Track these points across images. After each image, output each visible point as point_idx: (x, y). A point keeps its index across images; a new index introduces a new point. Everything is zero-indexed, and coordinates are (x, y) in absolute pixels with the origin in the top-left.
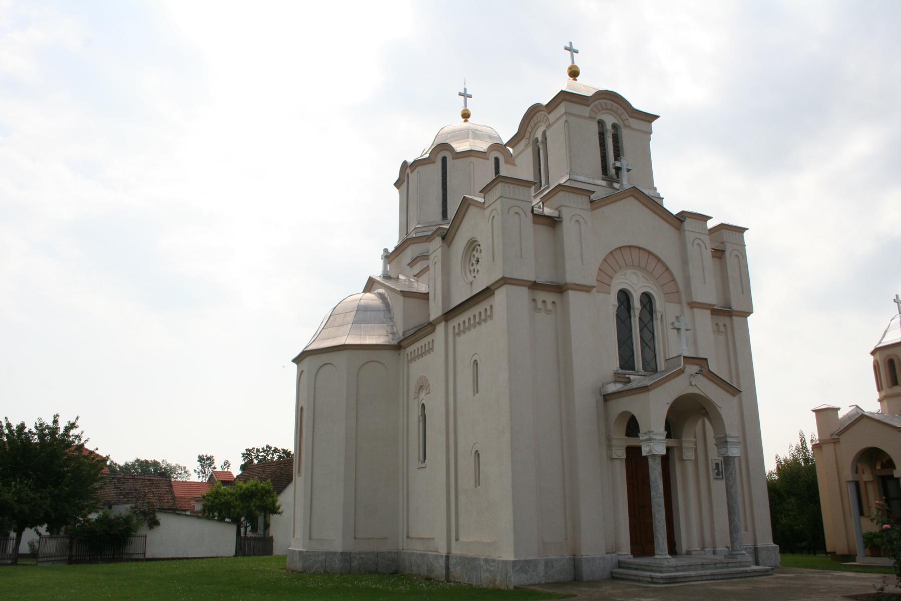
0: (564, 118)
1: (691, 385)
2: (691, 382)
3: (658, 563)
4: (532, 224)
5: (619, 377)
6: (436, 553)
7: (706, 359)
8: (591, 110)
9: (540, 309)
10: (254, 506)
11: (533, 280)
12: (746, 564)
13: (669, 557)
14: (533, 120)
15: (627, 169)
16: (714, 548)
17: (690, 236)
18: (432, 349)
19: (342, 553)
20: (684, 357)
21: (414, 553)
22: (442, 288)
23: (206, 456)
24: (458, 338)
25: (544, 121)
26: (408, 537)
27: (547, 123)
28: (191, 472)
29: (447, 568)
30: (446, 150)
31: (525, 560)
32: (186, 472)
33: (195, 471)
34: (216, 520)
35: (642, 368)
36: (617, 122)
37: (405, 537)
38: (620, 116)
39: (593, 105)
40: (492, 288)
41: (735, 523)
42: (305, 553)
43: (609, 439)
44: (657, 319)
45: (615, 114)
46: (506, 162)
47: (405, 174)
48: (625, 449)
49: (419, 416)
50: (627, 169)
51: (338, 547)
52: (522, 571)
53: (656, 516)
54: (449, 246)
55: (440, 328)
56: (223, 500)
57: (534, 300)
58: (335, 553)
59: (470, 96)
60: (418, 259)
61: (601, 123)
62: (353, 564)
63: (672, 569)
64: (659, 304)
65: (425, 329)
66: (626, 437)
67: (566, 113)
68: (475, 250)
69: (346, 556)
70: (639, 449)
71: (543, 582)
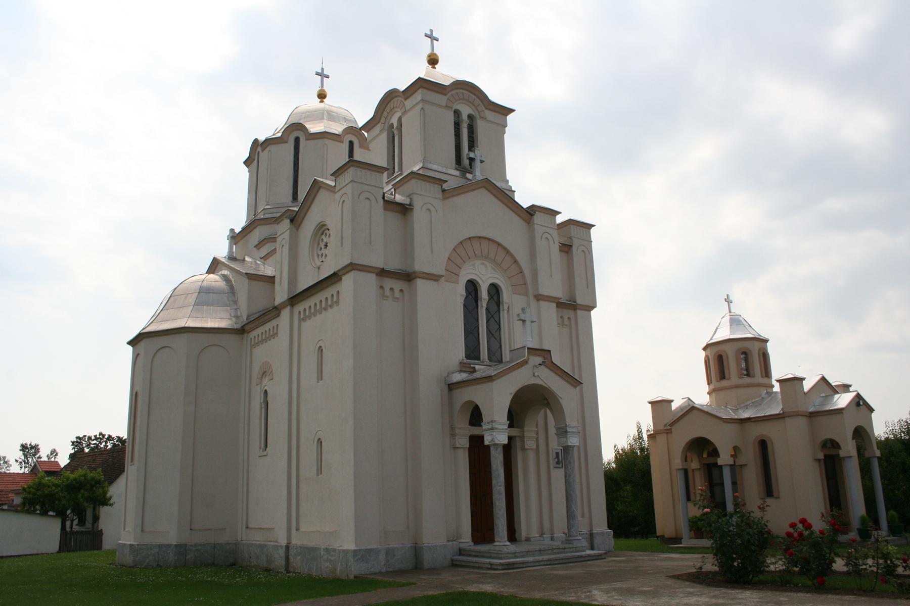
0: (420, 106)
1: (534, 376)
2: (534, 373)
3: (497, 549)
4: (382, 211)
5: (463, 366)
6: (276, 544)
7: (549, 351)
8: (448, 99)
9: (388, 297)
10: (82, 497)
11: (381, 266)
13: (509, 543)
14: (389, 105)
15: (481, 160)
16: (552, 534)
17: (539, 230)
18: (277, 334)
19: (176, 546)
20: (528, 348)
21: (253, 544)
22: (289, 272)
23: (30, 445)
24: (304, 325)
25: (400, 107)
26: (247, 527)
27: (403, 110)
28: (12, 462)
29: (287, 558)
30: (302, 131)
31: (366, 549)
32: (5, 462)
33: (16, 461)
34: (38, 514)
35: (487, 357)
36: (472, 112)
37: (244, 527)
38: (476, 107)
39: (450, 94)
40: (340, 273)
42: (137, 546)
43: (452, 428)
44: (503, 310)
45: (471, 105)
46: (361, 146)
47: (255, 153)
48: (468, 438)
49: (261, 403)
50: (481, 160)
51: (173, 539)
52: (363, 560)
53: (497, 504)
54: (297, 229)
55: (286, 313)
56: (46, 492)
57: (381, 287)
58: (169, 546)
59: (327, 77)
60: (266, 241)
61: (457, 113)
62: (187, 557)
63: (511, 555)
64: (506, 296)
65: (270, 313)
66: (470, 426)
67: (422, 100)
68: (324, 234)
69: (181, 549)
70: (481, 438)
71: (384, 571)
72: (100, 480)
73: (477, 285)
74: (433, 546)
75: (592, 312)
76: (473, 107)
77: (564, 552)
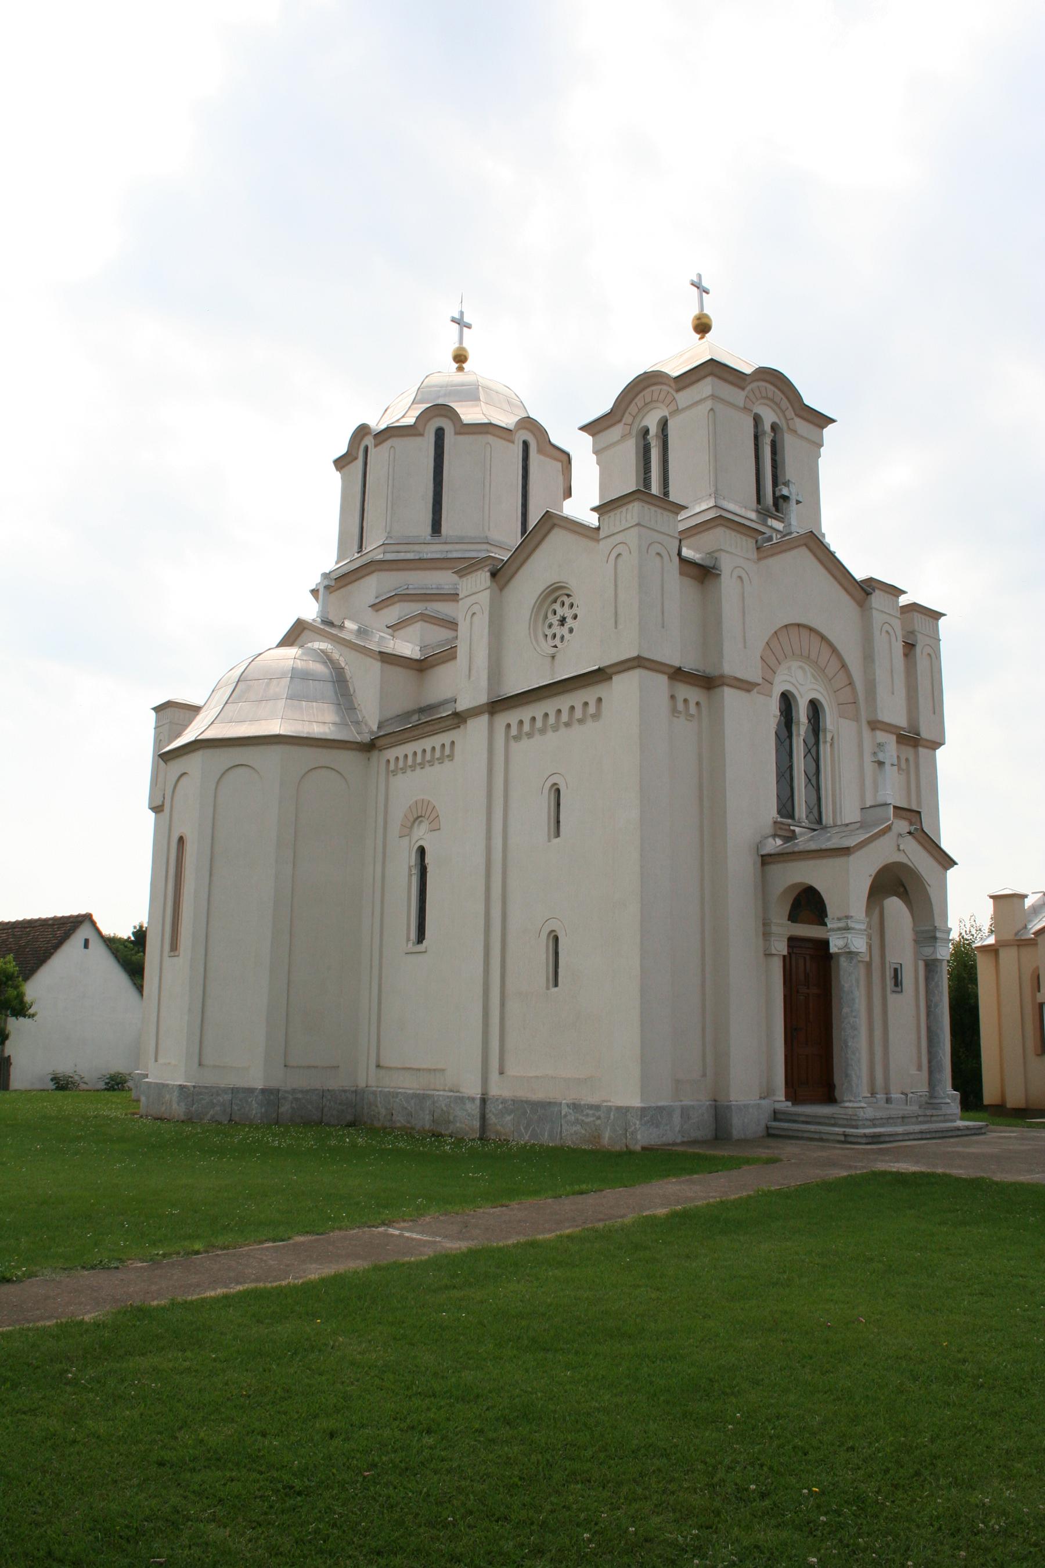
0: (709, 404)
1: (899, 850)
2: (899, 846)
3: (850, 1113)
4: (677, 575)
5: (781, 829)
6: (457, 1094)
7: (919, 813)
9: (680, 712)
11: (677, 664)
12: (951, 1118)
14: (642, 394)
15: (797, 501)
16: (886, 1094)
17: (877, 618)
19: (263, 1091)
20: (895, 807)
21: (398, 1094)
25: (667, 401)
26: (378, 1066)
27: (673, 407)
29: (483, 1118)
31: (657, 1107)
35: (804, 817)
36: (777, 421)
37: (373, 1066)
38: (783, 412)
39: (749, 388)
40: (609, 671)
41: (939, 1058)
42: (192, 1089)
43: (766, 924)
44: (825, 742)
45: (775, 407)
46: (540, 451)
47: (359, 445)
48: (786, 940)
50: (797, 501)
51: (257, 1082)
52: (653, 1124)
53: (850, 1044)
54: (501, 589)
58: (250, 1091)
59: (469, 326)
60: (396, 599)
61: (757, 420)
62: (282, 1110)
64: (830, 720)
65: (439, 722)
66: (790, 922)
67: (713, 397)
68: (559, 601)
69: (271, 1096)
70: (826, 943)
71: (679, 1141)
72: (13, 974)
73: (791, 699)
74: (745, 1106)
75: (937, 751)
76: (778, 411)
77: (931, 1122)
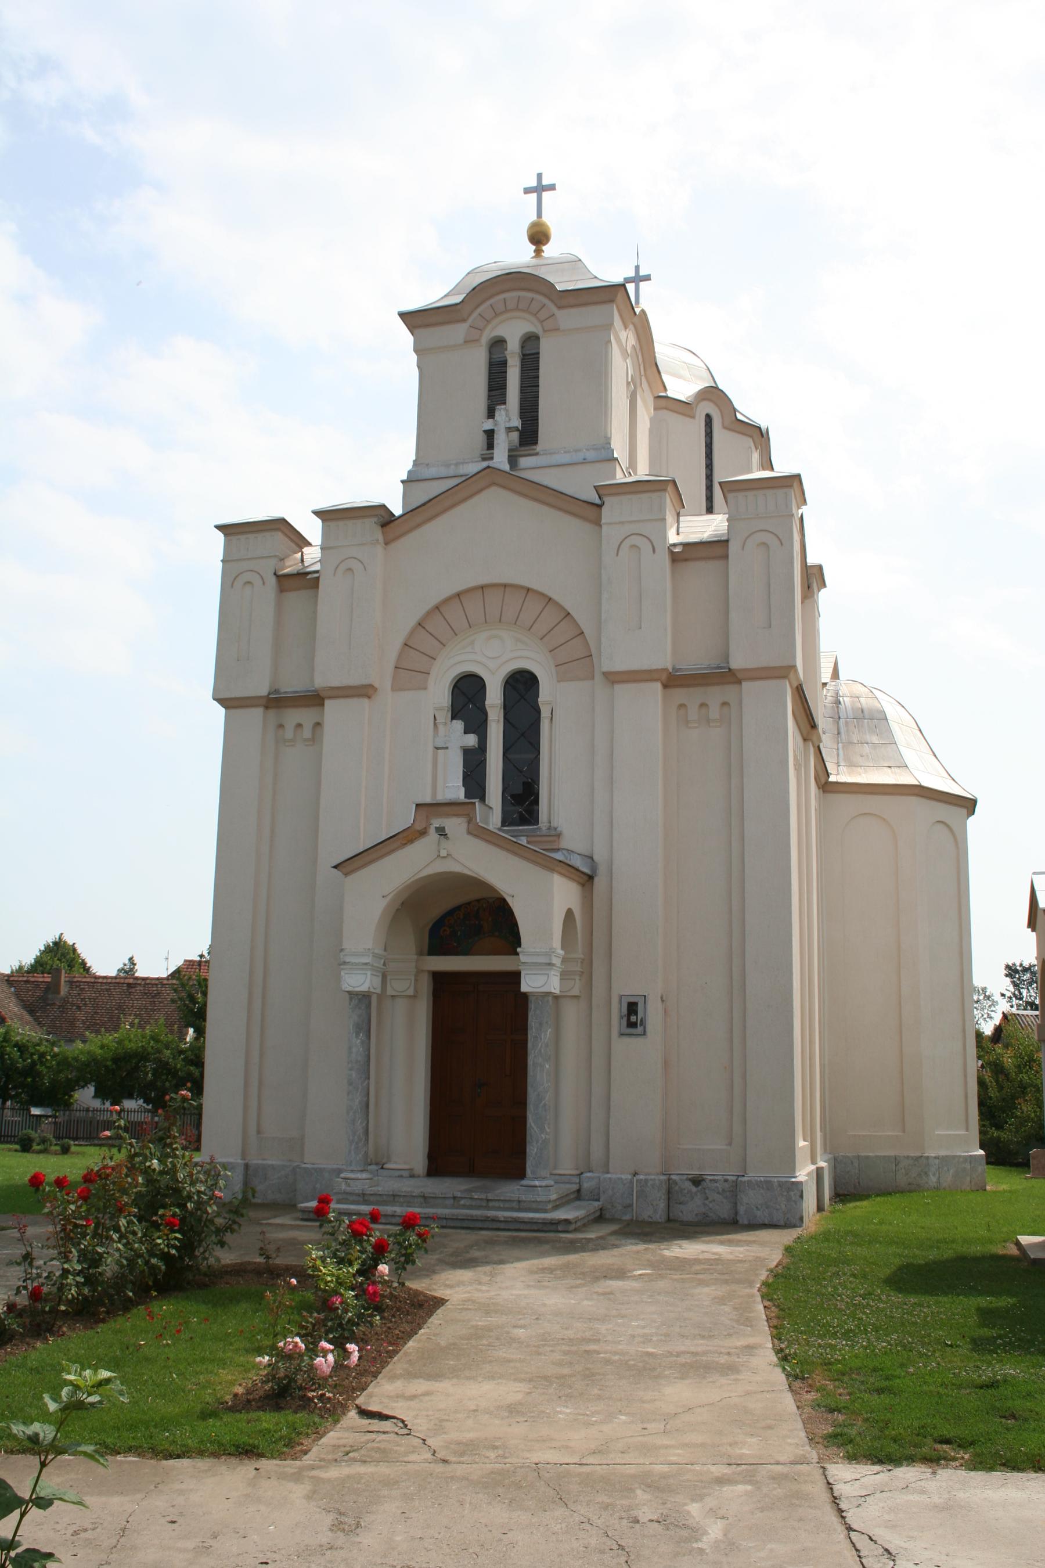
12: (534, 1206)
23: (1021, 965)
28: (997, 997)
32: (988, 998)
33: (1003, 995)
61: (498, 344)
63: (355, 1198)
74: (316, 1169)
77: (488, 1208)
